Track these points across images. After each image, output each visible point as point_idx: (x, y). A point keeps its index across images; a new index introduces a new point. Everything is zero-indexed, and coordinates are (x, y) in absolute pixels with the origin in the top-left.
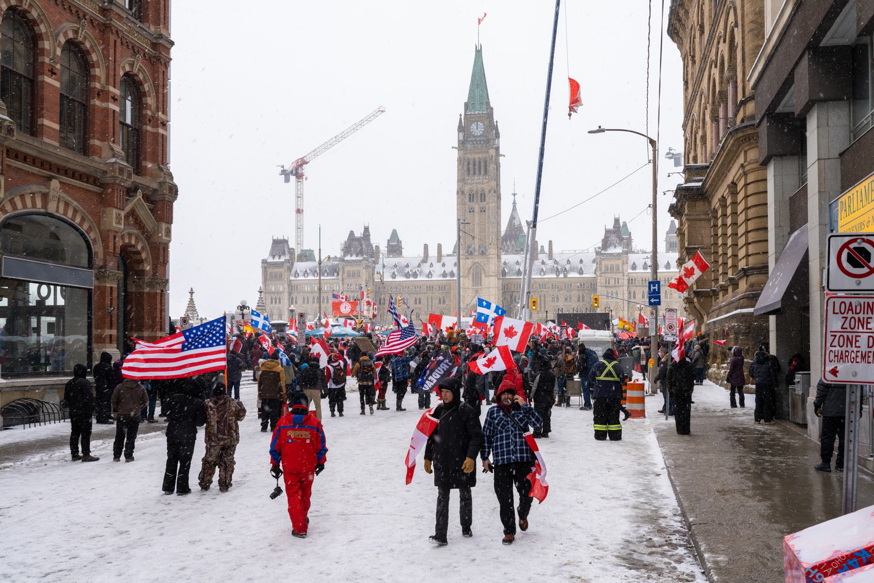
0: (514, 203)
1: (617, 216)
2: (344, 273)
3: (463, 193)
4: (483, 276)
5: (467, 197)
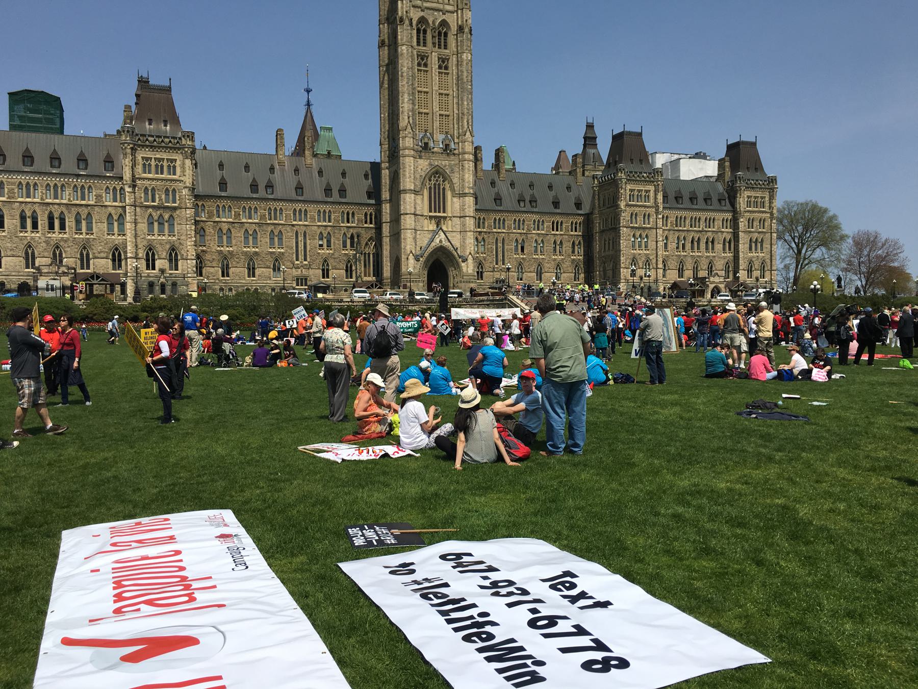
1: (590, 121)
4: (449, 194)
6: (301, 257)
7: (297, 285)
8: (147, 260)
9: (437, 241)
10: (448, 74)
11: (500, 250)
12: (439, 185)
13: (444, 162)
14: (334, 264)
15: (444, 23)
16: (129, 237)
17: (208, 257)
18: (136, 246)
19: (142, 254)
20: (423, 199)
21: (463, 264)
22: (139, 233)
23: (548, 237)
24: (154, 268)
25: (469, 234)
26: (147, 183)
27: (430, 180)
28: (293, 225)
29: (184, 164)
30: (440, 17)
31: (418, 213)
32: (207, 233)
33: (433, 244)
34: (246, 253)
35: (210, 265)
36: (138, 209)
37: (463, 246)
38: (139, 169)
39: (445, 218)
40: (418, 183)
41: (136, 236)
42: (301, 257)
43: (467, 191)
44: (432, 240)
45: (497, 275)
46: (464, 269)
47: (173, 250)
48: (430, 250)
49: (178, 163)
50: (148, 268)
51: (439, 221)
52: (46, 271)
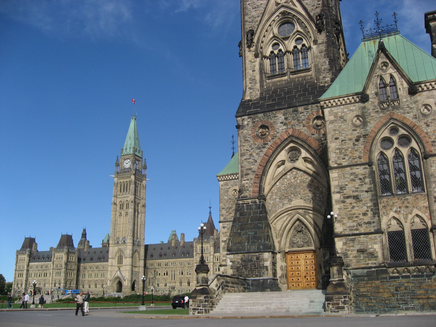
0: (210, 213)
9: (117, 275)
13: (122, 247)
16: (51, 278)
17: (85, 282)
19: (53, 283)
38: (56, 258)
40: (114, 255)
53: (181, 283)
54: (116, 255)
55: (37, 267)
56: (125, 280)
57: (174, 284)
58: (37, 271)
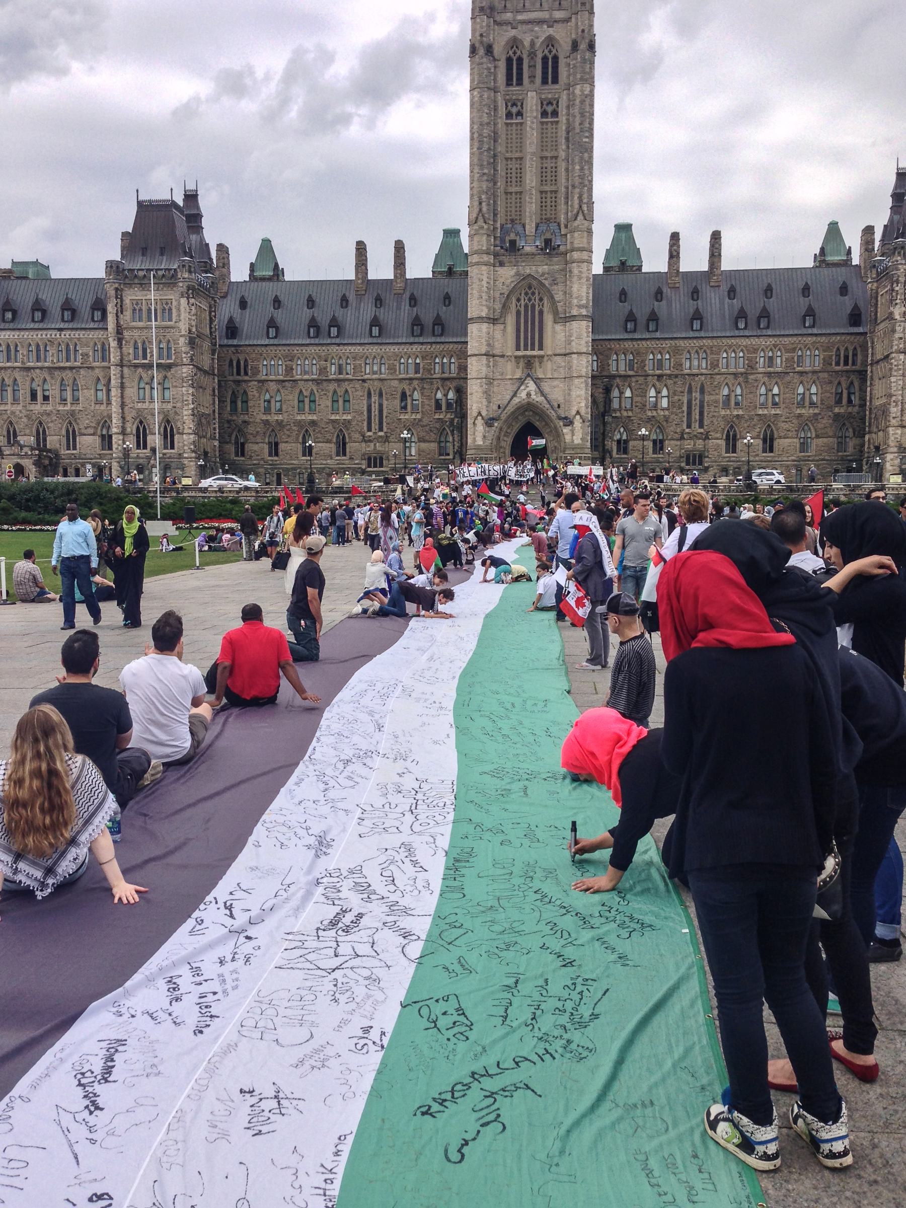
2: (121, 309)
3: (489, 50)
4: (548, 319)
5: (502, 65)
6: (375, 426)
7: (369, 466)
8: (138, 437)
9: (523, 395)
10: (557, 122)
11: (696, 403)
12: (533, 306)
13: (540, 268)
14: (422, 434)
15: (550, 42)
16: (115, 408)
17: (251, 429)
18: (123, 418)
19: (131, 428)
20: (504, 330)
21: (566, 430)
22: (127, 401)
23: (788, 378)
24: (145, 447)
25: (576, 381)
26: (136, 333)
27: (518, 300)
28: (364, 381)
29: (179, 304)
30: (544, 32)
31: (497, 352)
32: (250, 397)
33: (516, 400)
34: (299, 424)
35: (253, 440)
36: (126, 370)
37: (568, 402)
38: (128, 314)
39: (542, 357)
40: (498, 306)
41: (123, 405)
42: (375, 426)
43: (575, 312)
44: (515, 395)
45: (688, 445)
46: (568, 438)
47: (168, 422)
48: (510, 409)
49: (174, 303)
50: (138, 447)
51: (529, 363)
52: (8, 452)
53: (732, 442)
54: (505, 306)
55: (40, 351)
56: (569, 422)
57: (700, 444)
58: (17, 375)
